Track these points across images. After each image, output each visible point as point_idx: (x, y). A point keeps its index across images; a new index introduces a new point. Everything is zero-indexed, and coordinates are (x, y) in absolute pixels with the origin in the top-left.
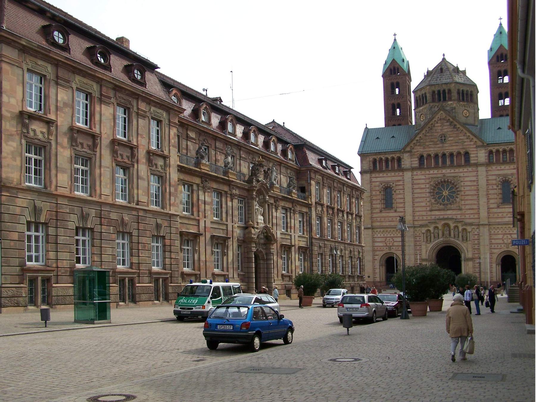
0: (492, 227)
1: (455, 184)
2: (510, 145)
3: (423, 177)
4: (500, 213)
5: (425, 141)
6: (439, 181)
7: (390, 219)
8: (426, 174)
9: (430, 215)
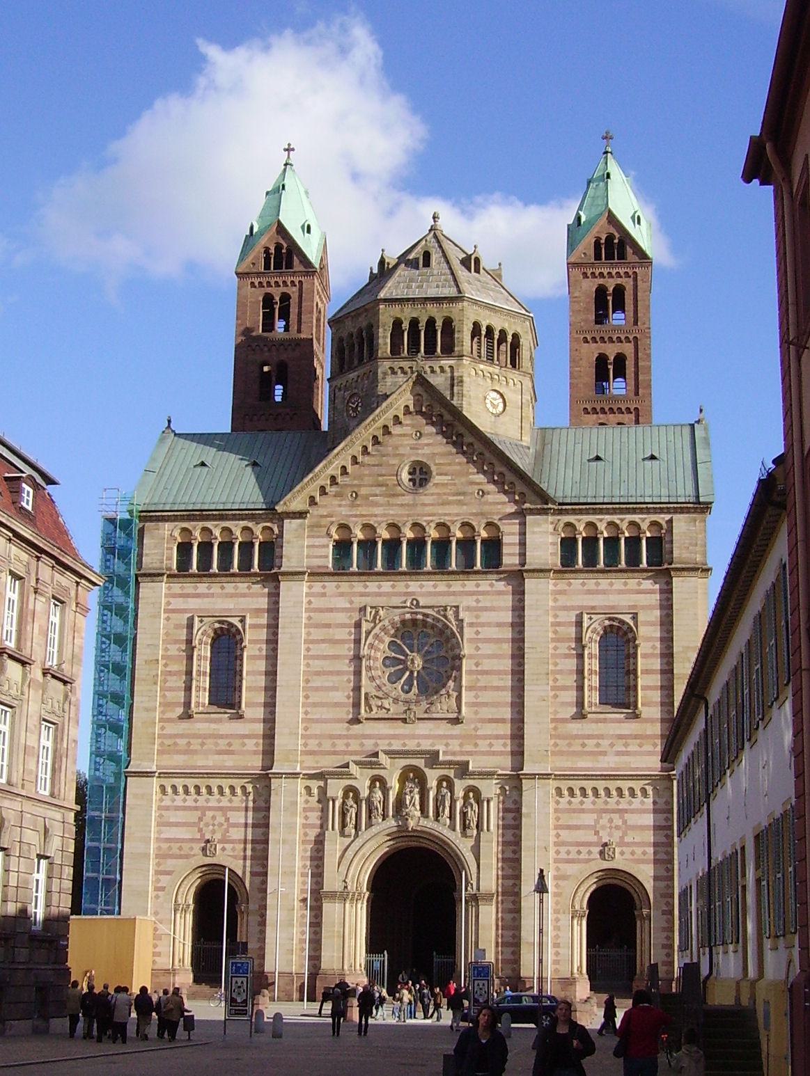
2: (629, 513)
3: (343, 603)
4: (589, 737)
5: (356, 482)
6: (397, 619)
7: (223, 744)
8: (354, 594)
9: (356, 737)
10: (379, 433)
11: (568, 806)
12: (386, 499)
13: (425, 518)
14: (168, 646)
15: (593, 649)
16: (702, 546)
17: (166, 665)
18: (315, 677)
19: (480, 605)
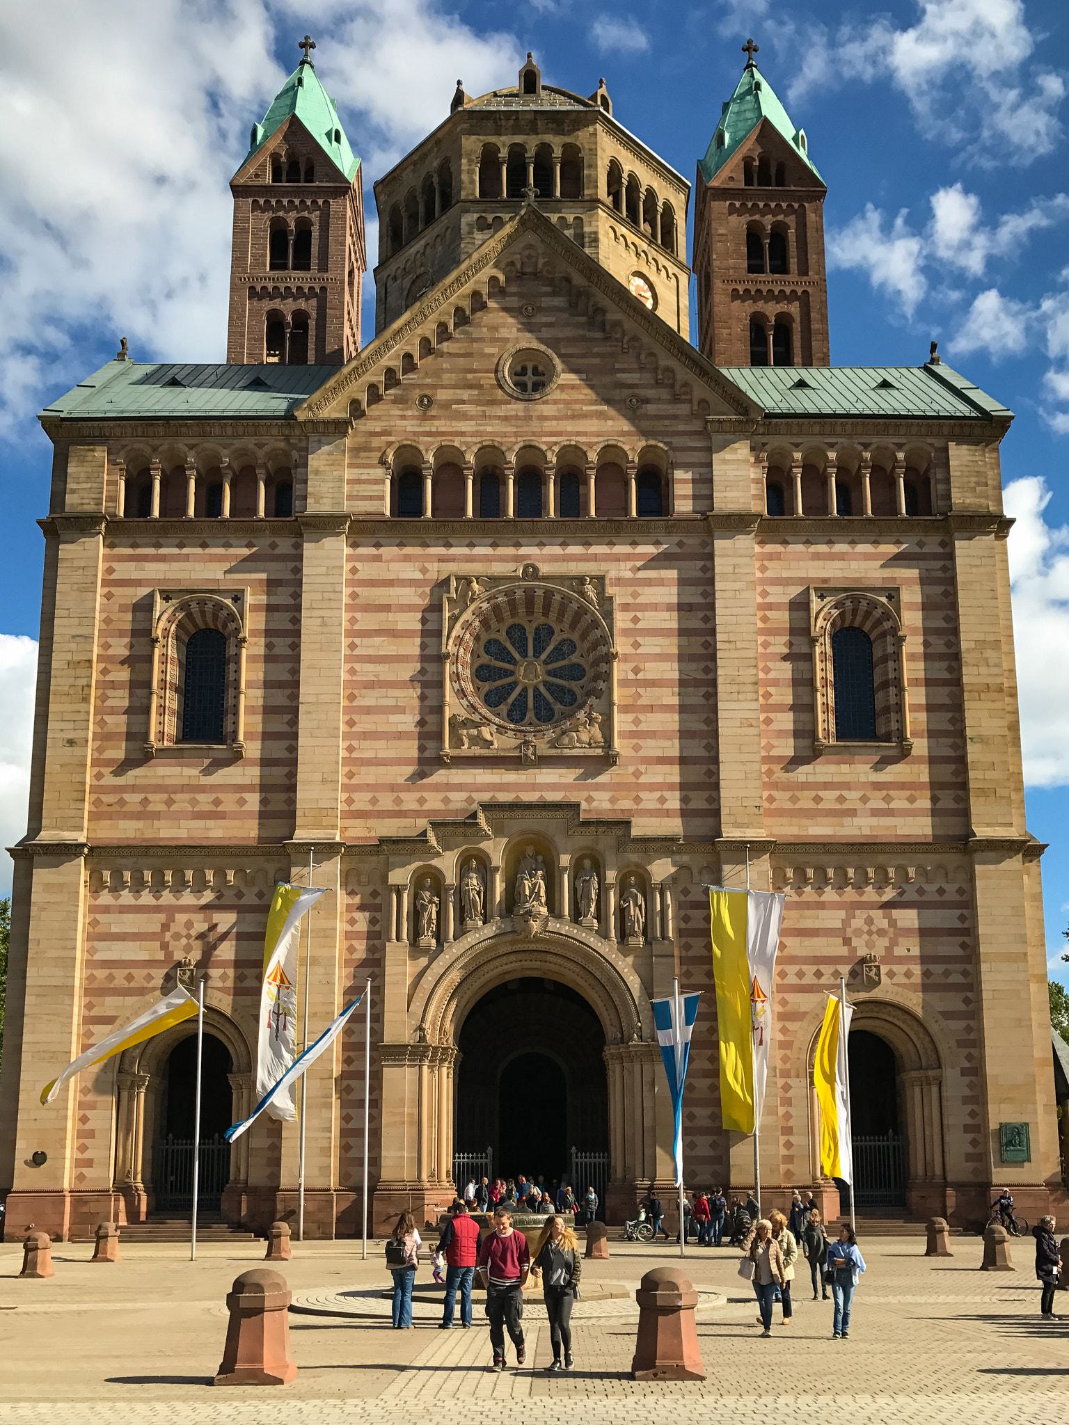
3: (410, 572)
5: (429, 381)
7: (205, 800)
10: (467, 305)
12: (479, 408)
13: (544, 439)
14: (109, 640)
15: (823, 648)
16: (994, 488)
17: (104, 672)
18: (364, 691)
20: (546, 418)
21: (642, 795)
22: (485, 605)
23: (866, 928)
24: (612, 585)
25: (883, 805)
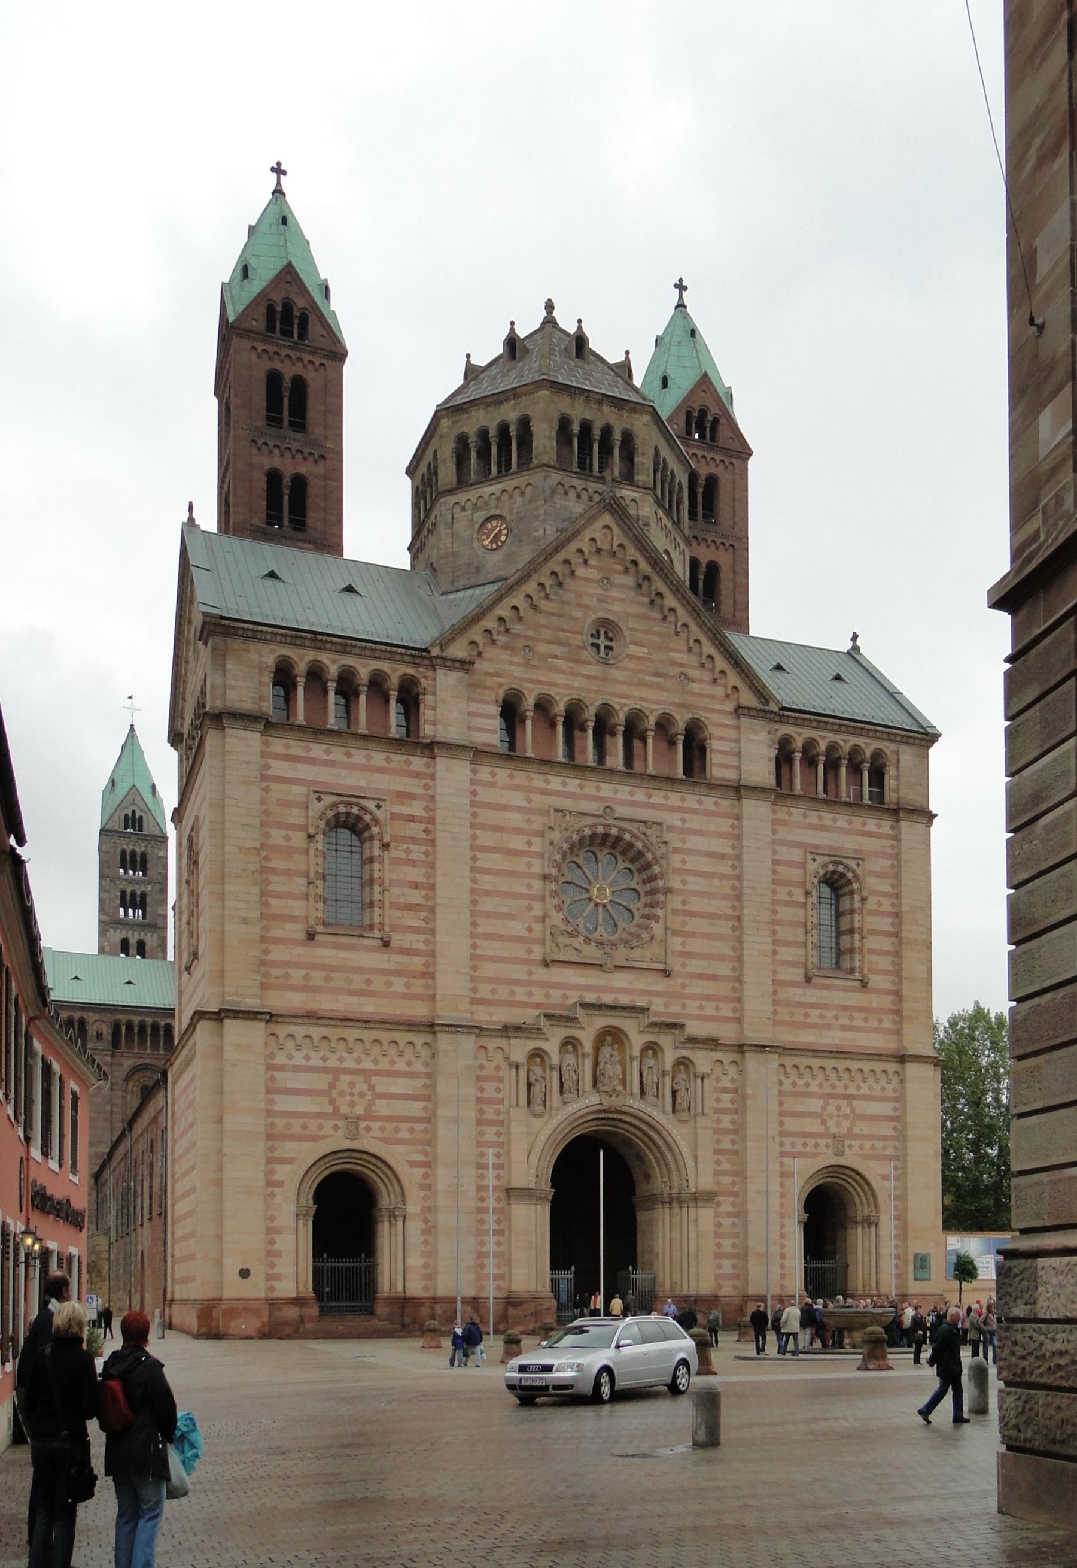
0: (789, 1061)
1: (649, 856)
3: (518, 800)
6: (587, 832)
7: (358, 983)
8: (531, 789)
11: (791, 1088)
13: (617, 700)
19: (687, 825)
20: (619, 682)
21: (687, 1002)
22: (575, 837)
23: (836, 1113)
24: (668, 831)
25: (847, 1022)
